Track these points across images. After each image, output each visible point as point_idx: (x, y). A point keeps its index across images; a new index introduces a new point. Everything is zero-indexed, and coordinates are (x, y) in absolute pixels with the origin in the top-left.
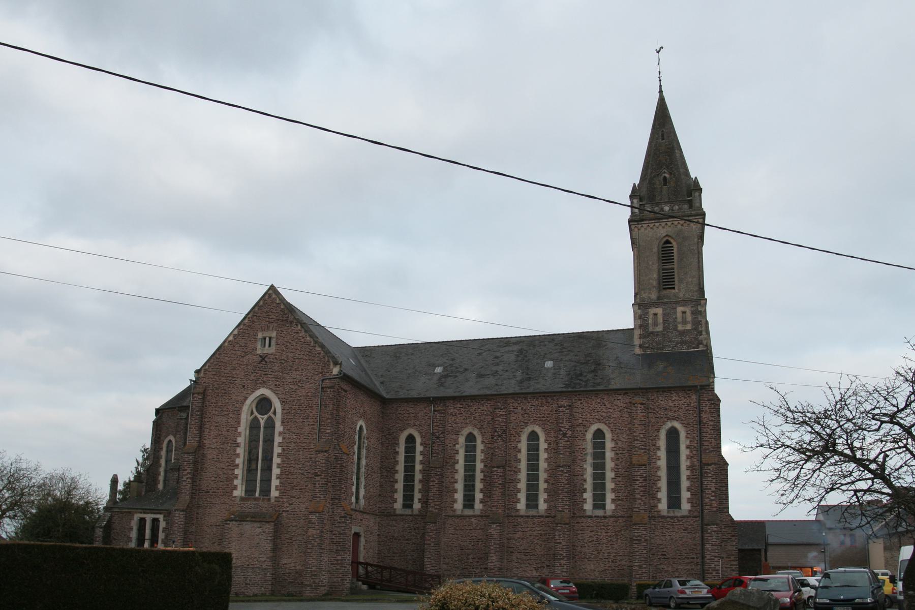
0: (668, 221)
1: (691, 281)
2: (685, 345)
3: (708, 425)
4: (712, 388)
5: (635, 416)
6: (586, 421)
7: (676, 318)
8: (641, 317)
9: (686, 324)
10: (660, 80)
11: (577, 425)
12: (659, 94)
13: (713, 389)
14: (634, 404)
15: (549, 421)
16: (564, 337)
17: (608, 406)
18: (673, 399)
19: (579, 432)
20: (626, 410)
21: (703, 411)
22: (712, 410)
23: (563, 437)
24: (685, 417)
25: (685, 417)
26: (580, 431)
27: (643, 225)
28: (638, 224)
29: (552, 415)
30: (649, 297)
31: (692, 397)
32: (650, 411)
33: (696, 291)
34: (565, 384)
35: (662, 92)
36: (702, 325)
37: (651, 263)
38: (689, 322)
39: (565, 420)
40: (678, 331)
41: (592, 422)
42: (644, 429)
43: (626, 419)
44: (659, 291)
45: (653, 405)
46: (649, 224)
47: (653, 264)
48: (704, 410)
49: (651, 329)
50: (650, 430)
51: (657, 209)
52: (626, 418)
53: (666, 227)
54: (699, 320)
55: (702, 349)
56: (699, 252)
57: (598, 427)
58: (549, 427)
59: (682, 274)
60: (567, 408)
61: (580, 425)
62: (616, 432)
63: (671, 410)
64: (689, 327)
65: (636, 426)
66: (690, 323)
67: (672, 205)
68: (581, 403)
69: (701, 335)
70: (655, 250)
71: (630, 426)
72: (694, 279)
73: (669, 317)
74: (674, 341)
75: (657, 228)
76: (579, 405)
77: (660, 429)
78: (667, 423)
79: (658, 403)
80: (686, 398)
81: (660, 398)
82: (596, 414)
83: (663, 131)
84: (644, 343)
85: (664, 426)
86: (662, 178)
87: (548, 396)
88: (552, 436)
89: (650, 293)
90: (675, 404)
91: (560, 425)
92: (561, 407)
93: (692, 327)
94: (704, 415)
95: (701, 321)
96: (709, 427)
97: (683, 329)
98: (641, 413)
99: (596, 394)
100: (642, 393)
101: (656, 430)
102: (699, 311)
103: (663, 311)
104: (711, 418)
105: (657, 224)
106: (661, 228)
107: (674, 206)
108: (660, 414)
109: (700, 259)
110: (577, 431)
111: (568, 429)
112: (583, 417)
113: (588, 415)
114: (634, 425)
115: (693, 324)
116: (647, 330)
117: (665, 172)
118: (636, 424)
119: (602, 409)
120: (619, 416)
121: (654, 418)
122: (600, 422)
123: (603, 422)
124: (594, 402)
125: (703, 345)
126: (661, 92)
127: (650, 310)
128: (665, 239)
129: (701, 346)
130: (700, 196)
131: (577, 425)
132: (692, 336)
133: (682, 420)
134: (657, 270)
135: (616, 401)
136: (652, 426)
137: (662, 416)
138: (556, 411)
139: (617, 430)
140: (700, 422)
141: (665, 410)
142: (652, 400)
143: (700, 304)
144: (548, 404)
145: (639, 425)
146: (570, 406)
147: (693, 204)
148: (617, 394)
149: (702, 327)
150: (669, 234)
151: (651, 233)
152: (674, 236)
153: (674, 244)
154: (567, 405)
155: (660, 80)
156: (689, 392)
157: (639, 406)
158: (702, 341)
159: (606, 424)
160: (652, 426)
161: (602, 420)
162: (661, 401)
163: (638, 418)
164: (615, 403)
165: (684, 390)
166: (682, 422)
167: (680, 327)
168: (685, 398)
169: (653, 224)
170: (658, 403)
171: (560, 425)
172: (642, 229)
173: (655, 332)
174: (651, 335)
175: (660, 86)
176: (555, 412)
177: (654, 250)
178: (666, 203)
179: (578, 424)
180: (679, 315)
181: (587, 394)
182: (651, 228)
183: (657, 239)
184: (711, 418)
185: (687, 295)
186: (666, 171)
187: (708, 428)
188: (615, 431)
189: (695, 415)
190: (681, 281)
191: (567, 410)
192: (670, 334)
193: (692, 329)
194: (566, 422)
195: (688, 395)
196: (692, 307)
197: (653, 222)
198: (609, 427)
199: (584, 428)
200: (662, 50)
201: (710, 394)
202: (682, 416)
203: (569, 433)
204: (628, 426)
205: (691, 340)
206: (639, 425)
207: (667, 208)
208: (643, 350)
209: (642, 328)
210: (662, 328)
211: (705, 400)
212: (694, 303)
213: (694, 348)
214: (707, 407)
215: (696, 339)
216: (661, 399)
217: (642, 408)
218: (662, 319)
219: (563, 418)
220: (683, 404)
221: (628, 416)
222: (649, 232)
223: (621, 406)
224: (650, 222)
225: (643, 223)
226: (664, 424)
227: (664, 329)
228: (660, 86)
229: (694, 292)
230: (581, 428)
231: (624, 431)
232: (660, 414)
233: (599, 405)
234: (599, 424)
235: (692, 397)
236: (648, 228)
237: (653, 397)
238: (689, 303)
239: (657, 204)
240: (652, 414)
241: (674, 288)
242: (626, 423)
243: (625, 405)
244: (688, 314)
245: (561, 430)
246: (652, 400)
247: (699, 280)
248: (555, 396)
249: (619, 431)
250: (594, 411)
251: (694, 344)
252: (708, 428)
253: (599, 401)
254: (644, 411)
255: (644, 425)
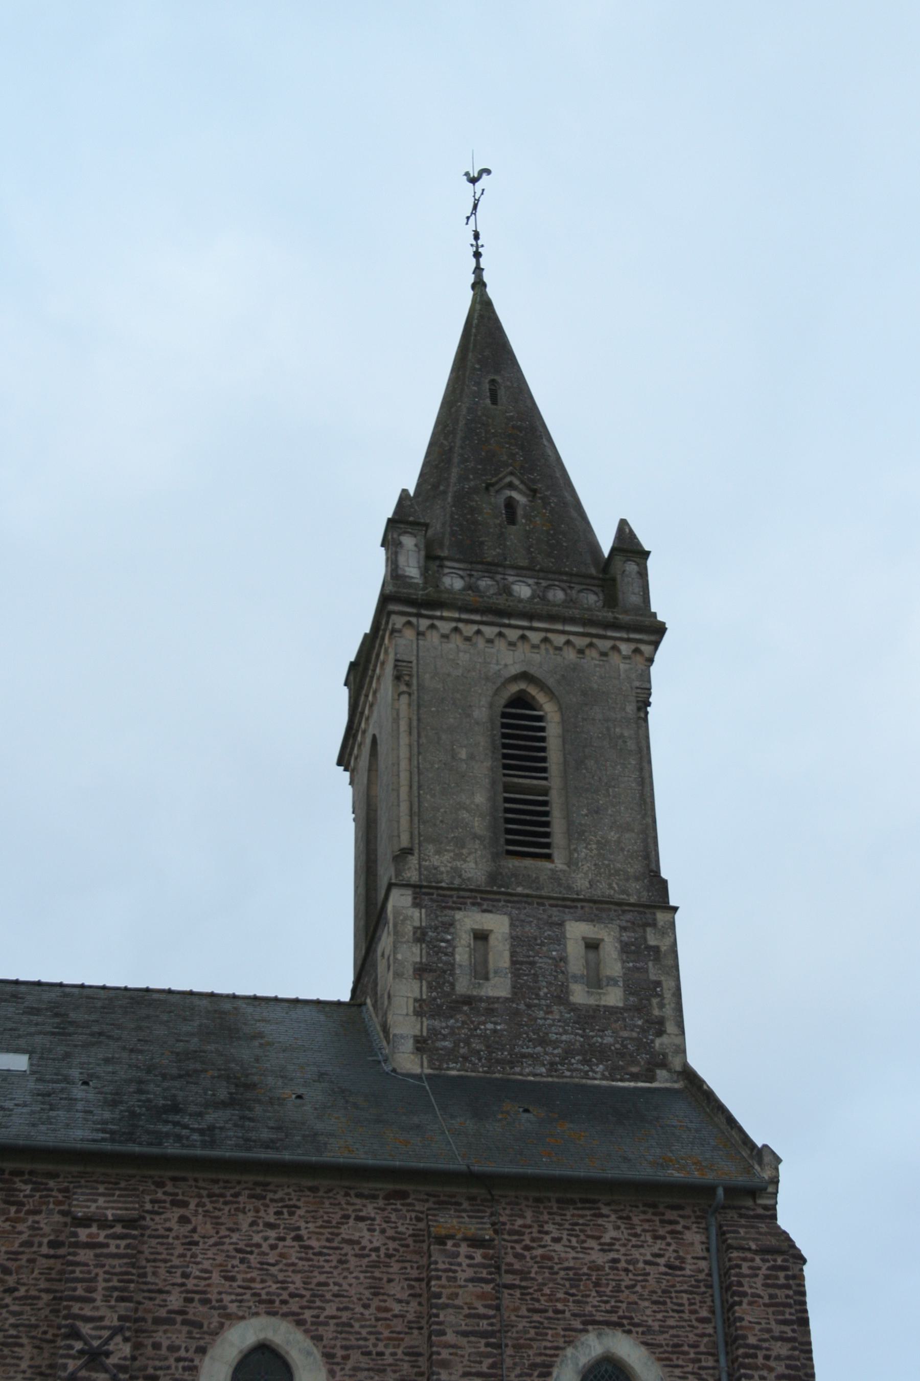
0: (531, 629)
1: (619, 841)
2: (600, 1061)
3: (767, 1358)
4: (766, 1208)
5: (445, 1292)
6: (205, 1302)
7: (564, 959)
8: (424, 934)
9: (600, 987)
10: (477, 255)
11: (157, 1321)
12: (471, 293)
13: (771, 1214)
14: (441, 1241)
15: (10, 1291)
16: (66, 995)
17: (314, 1243)
18: (606, 1239)
19: (164, 1351)
20: (396, 1267)
21: (744, 1294)
22: (781, 1293)
23: (85, 1366)
24: (659, 1316)
25: (659, 1316)
26: (173, 1348)
27: (438, 623)
28: (419, 615)
29: (31, 1261)
30: (457, 871)
31: (688, 1236)
32: (508, 1279)
33: (637, 879)
34: (104, 1131)
35: (484, 285)
36: (661, 996)
37: (463, 754)
38: (612, 981)
39: (101, 1285)
40: (574, 1008)
41: (233, 1308)
42: (488, 1355)
43: (397, 1308)
44: (495, 857)
45: (517, 1256)
46: (461, 625)
47: (471, 757)
48: (746, 1288)
49: (463, 986)
50: (508, 1362)
51: (488, 587)
52: (400, 1301)
53: (522, 648)
54: (653, 977)
55: (668, 1085)
56: (640, 750)
57: (262, 1336)
58: (12, 1320)
59: (585, 812)
60: (118, 1229)
61: (171, 1322)
62: (350, 1364)
63: (597, 1284)
64: (614, 997)
65: (450, 1337)
66: (616, 984)
67: (544, 583)
68: (184, 1220)
69: (660, 1033)
70: (481, 713)
71: (416, 1339)
72: (627, 836)
73: (537, 954)
74: (555, 1044)
75: (490, 641)
76: (173, 1224)
77: (551, 1366)
78: (584, 1337)
79: (540, 1251)
80: (663, 1238)
81: (549, 1227)
82: (254, 1274)
83: (493, 382)
84: (433, 1032)
85: (569, 1351)
86: (501, 500)
87: (19, 1173)
88: (24, 1365)
89: (459, 856)
90: (615, 1261)
91: (76, 1308)
92: (86, 1222)
93: (626, 1000)
94: (747, 1313)
95: (658, 983)
96: (772, 1363)
97: (592, 1001)
98: (472, 1280)
99: (256, 1184)
100: (471, 1199)
101: (534, 1366)
102: (649, 948)
103: (512, 925)
104: (777, 1329)
105: (489, 631)
106: (501, 644)
107: (548, 587)
108: (551, 1298)
109: (645, 765)
110: (157, 1346)
111: (116, 1331)
112: (191, 1283)
113: (216, 1277)
114: (443, 1333)
115: (630, 989)
116: (447, 988)
117: (510, 486)
118: (449, 1331)
119: (282, 1255)
120: (367, 1293)
121: (523, 1311)
122: (274, 1314)
123: (285, 1315)
124: (244, 1221)
125: (669, 1070)
126: (479, 285)
127: (459, 915)
128: (514, 688)
129: (661, 1073)
130: (643, 574)
131: (157, 1321)
132: (625, 1034)
133: (649, 1330)
134: (486, 782)
135: (351, 1221)
136: (518, 1347)
137: (560, 1306)
138: (52, 1244)
139: (355, 1356)
140: (733, 1340)
141: (575, 1281)
142: (512, 1232)
143: (654, 925)
144: (13, 1209)
145: (465, 1334)
146: (129, 1223)
147: (620, 596)
148: (359, 1195)
149: (661, 1006)
150: (533, 671)
151: (467, 656)
152: (551, 682)
153: (549, 708)
154: (118, 1220)
155: (477, 255)
156: (671, 1215)
157: (464, 1249)
158: (665, 1055)
159: (300, 1323)
160: (518, 1347)
161: (283, 1302)
162: (557, 1240)
163: (457, 1302)
164: (346, 1231)
165: (654, 1206)
166: (648, 1338)
167: (579, 995)
168: (656, 1237)
169: (475, 628)
170: (540, 1251)
171: (76, 1308)
172: (433, 638)
173: (481, 999)
174: (466, 1008)
175: (478, 270)
176: (45, 1250)
177: (476, 714)
178: (522, 571)
179: (163, 1313)
180: (574, 950)
181: (216, 1181)
182: (468, 639)
183: (487, 679)
184: (777, 1329)
185: (603, 885)
186: (517, 482)
187: (771, 1369)
188: (346, 1358)
189: (704, 1313)
190: (575, 833)
191: (113, 1243)
192: (541, 1014)
193: (625, 1009)
194: (106, 1299)
195: (669, 1228)
196: (623, 929)
197: (477, 618)
198: (317, 1339)
199: (190, 1336)
200: (484, 176)
201: (763, 1228)
202: (647, 1313)
203: (121, 1350)
204: (408, 1341)
205: (625, 1047)
206: (465, 1334)
207: (523, 591)
208: (430, 1061)
209: (429, 977)
210: (509, 986)
211: (749, 1249)
212: (629, 916)
213: (635, 1077)
214: (759, 1281)
215: (644, 1046)
216: (556, 1234)
217: (478, 1259)
218: (507, 955)
219: (94, 1279)
220: (647, 1262)
221: (404, 1296)
222: (458, 650)
223: (377, 1250)
224: (464, 616)
225: (438, 613)
226: (569, 1343)
227: (515, 994)
228: (478, 270)
229: (627, 880)
230: (178, 1336)
231: (389, 1360)
232: (551, 1298)
233: (272, 1234)
234: (264, 1320)
235: (688, 1236)
236: (457, 639)
237: (520, 1222)
238: (612, 914)
239: (492, 568)
240: (518, 1293)
241: (548, 857)
242: (399, 1325)
243: (392, 1245)
244: (610, 952)
245: (75, 1334)
246: (512, 1232)
247: (645, 841)
248: (54, 1176)
249: (364, 1362)
250: (242, 1261)
251: (634, 1062)
252: (771, 1369)
253: (272, 1219)
254: (484, 1274)
255: (484, 1334)
